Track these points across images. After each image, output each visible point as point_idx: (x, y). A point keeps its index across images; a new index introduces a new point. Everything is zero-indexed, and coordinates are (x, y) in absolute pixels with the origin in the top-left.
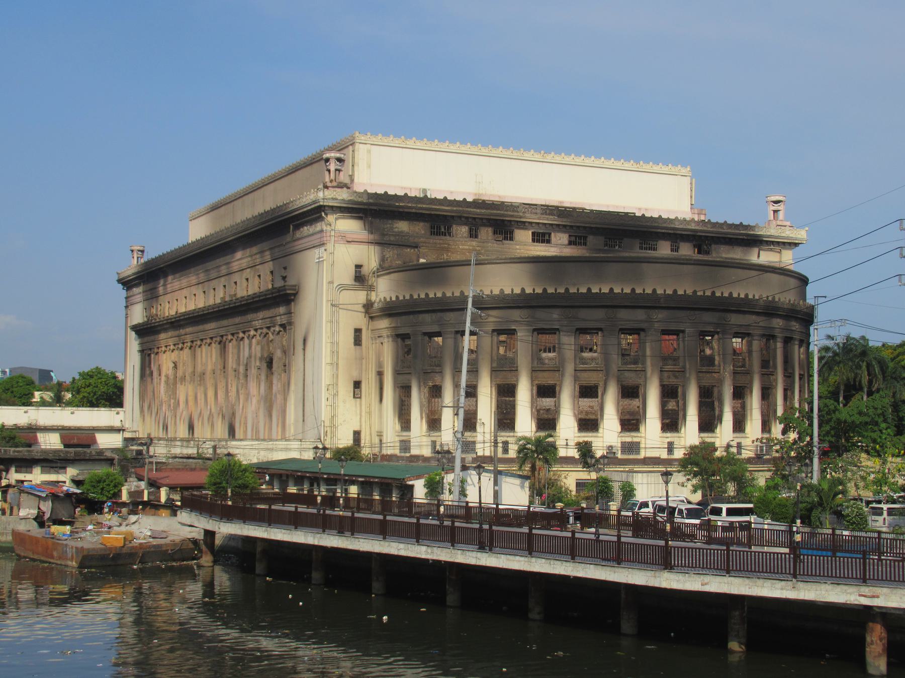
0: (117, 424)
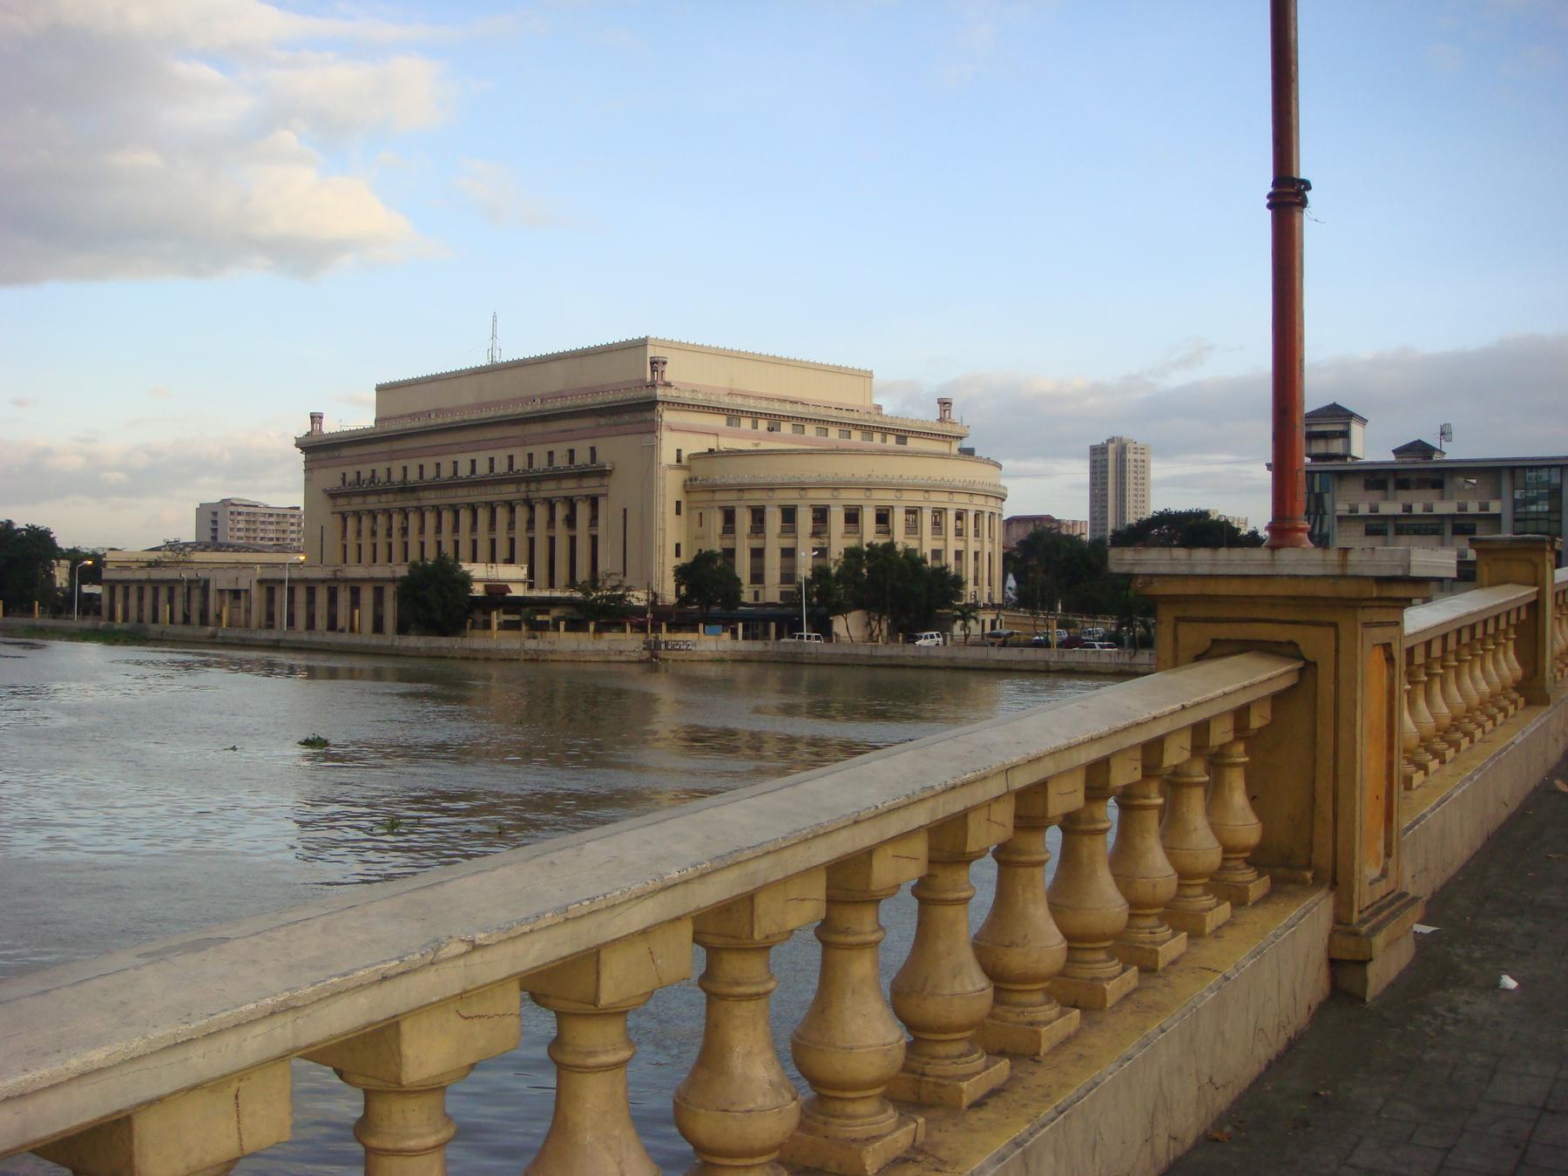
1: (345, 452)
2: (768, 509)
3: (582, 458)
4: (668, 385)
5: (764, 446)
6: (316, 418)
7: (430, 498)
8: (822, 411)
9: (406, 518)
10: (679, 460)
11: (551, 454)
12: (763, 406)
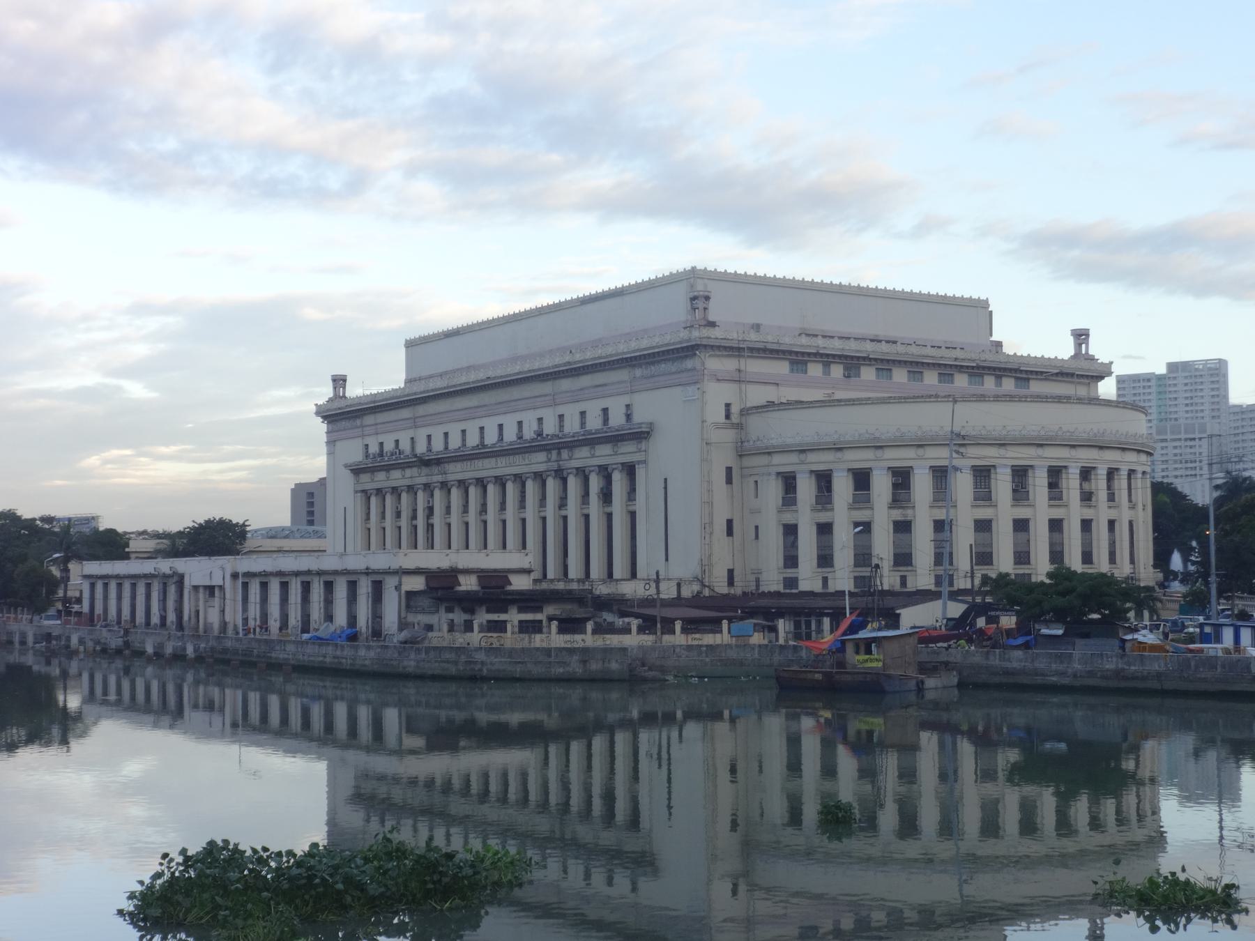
0: (526, 566)
1: (369, 420)
2: (835, 474)
3: (617, 419)
4: (712, 324)
5: (840, 395)
6: (339, 381)
7: (456, 472)
8: (914, 350)
9: (432, 496)
10: (728, 416)
11: (583, 414)
12: (835, 346)
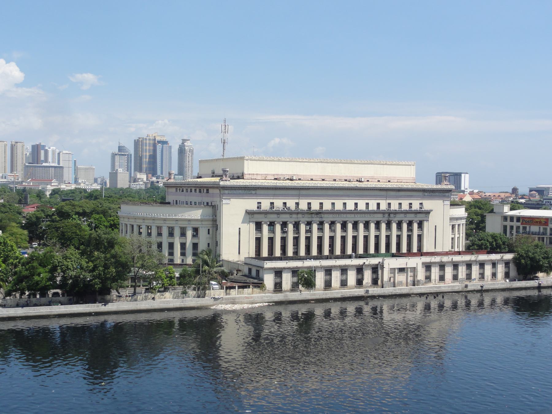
1: (258, 192)
